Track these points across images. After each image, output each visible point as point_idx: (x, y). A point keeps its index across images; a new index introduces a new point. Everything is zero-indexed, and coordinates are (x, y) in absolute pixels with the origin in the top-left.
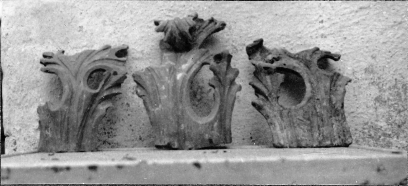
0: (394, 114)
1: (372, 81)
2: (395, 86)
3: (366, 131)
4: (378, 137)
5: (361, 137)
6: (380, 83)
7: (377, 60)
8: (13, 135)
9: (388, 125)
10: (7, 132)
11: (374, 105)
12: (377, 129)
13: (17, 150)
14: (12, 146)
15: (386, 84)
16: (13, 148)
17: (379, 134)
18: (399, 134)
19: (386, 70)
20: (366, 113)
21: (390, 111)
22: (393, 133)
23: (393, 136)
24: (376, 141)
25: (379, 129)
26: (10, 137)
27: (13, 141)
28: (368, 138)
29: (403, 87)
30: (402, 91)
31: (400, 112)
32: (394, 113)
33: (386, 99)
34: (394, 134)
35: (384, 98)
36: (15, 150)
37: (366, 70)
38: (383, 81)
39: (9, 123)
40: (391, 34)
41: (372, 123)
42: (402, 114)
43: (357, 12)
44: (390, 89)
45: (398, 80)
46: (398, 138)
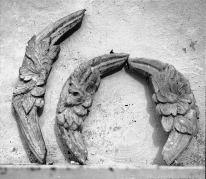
3: (193, 158)
4: (198, 162)
6: (201, 132)
11: (197, 144)
17: (200, 160)
20: (192, 148)
25: (199, 157)
35: (203, 140)
38: (202, 131)
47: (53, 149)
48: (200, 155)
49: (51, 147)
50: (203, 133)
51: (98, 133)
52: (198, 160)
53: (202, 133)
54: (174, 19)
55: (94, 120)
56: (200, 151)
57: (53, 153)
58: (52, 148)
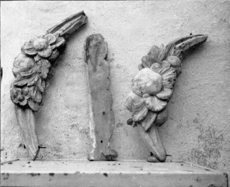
0: (208, 145)
2: (209, 130)
3: (193, 153)
4: (199, 157)
6: (201, 128)
8: (5, 149)
10: (2, 148)
12: (200, 153)
13: (7, 158)
14: (4, 156)
15: (204, 129)
16: (5, 157)
18: (211, 156)
19: (205, 122)
21: (206, 143)
22: (207, 155)
24: (198, 159)
26: (4, 151)
27: (6, 153)
31: (211, 144)
33: (204, 137)
35: (203, 136)
36: (6, 158)
37: (194, 121)
39: (3, 143)
41: (196, 149)
42: (212, 145)
43: (190, 90)
44: (206, 131)
46: (210, 157)
47: (58, 145)
49: (56, 142)
54: (174, 20)
57: (58, 149)
58: (57, 143)
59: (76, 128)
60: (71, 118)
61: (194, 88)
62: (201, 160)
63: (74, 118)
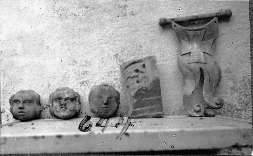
1: (229, 77)
2: (243, 81)
4: (233, 111)
5: (223, 111)
6: (234, 78)
7: (232, 65)
9: (240, 103)
11: (230, 92)
15: (238, 79)
17: (234, 109)
20: (226, 96)
21: (240, 95)
23: (243, 110)
24: (232, 113)
28: (227, 111)
29: (248, 81)
30: (248, 83)
31: (246, 95)
32: (243, 96)
33: (238, 88)
34: (243, 109)
35: (237, 88)
38: (236, 78)
40: (241, 49)
41: (229, 102)
42: (248, 97)
44: (240, 82)
45: (245, 77)
46: (245, 111)
48: (234, 103)
50: (237, 80)
51: (117, 84)
52: (231, 109)
53: (236, 80)
55: (111, 72)
56: (234, 99)
59: (87, 84)
60: (80, 74)
61: (225, 34)
62: (235, 114)
63: (83, 74)
